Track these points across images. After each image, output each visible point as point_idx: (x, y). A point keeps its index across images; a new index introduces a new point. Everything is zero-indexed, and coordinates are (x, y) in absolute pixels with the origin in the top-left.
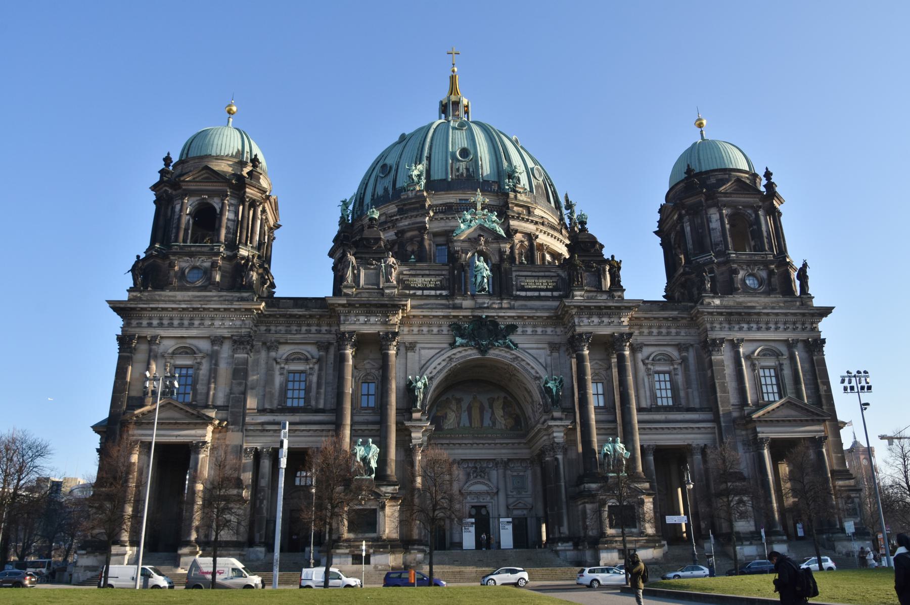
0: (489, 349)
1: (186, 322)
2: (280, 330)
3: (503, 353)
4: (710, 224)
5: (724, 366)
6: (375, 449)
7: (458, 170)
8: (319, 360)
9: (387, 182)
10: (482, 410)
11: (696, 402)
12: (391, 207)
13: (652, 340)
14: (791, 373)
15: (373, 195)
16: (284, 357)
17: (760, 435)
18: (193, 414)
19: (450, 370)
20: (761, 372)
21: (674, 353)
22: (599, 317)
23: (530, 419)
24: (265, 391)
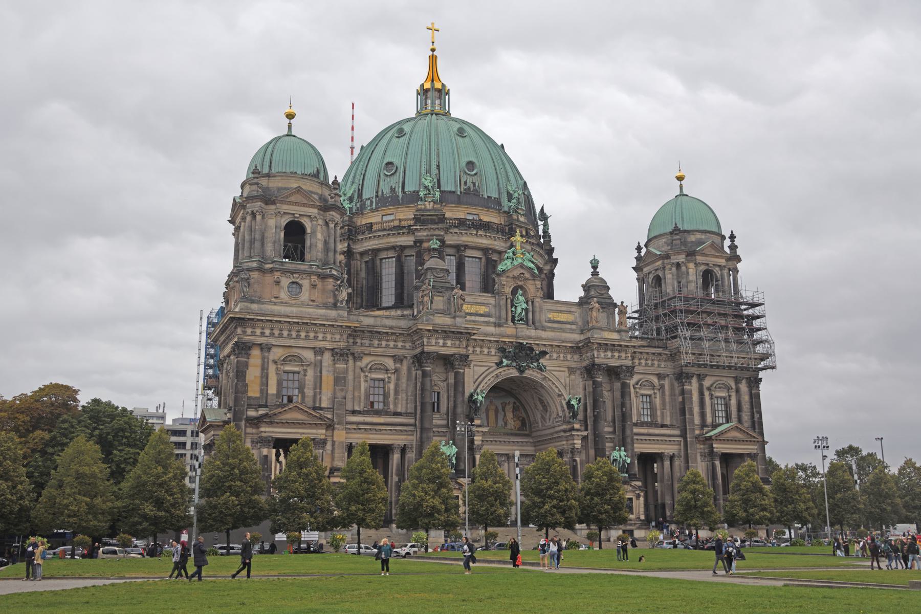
1: (294, 334)
6: (454, 450)
7: (466, 183)
9: (395, 181)
10: (497, 412)
11: (668, 422)
12: (399, 209)
14: (735, 402)
15: (377, 192)
16: (369, 367)
17: (715, 450)
18: (315, 416)
20: (716, 399)
21: (655, 380)
22: (612, 352)
23: (538, 423)
24: (354, 395)
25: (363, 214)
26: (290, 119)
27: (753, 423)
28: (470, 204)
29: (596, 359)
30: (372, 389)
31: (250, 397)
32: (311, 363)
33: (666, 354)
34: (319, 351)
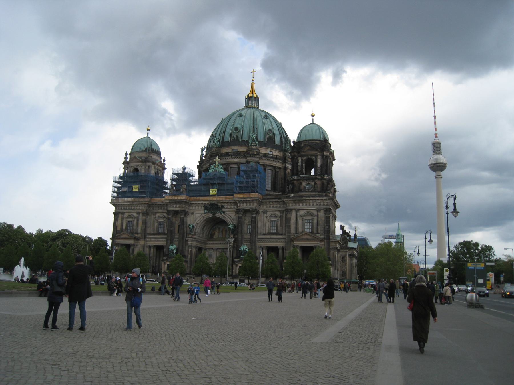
0: (215, 214)
1: (130, 208)
2: (156, 209)
3: (220, 215)
4: (298, 163)
5: (290, 219)
6: (175, 246)
7: (233, 137)
8: (167, 218)
9: (212, 141)
13: (270, 209)
15: (209, 147)
16: (157, 217)
17: (295, 244)
19: (204, 221)
21: (278, 214)
25: (207, 156)
26: (148, 131)
27: (325, 230)
28: (234, 146)
29: (238, 207)
30: (160, 225)
31: (118, 231)
32: (136, 217)
33: (282, 201)
34: (138, 213)
